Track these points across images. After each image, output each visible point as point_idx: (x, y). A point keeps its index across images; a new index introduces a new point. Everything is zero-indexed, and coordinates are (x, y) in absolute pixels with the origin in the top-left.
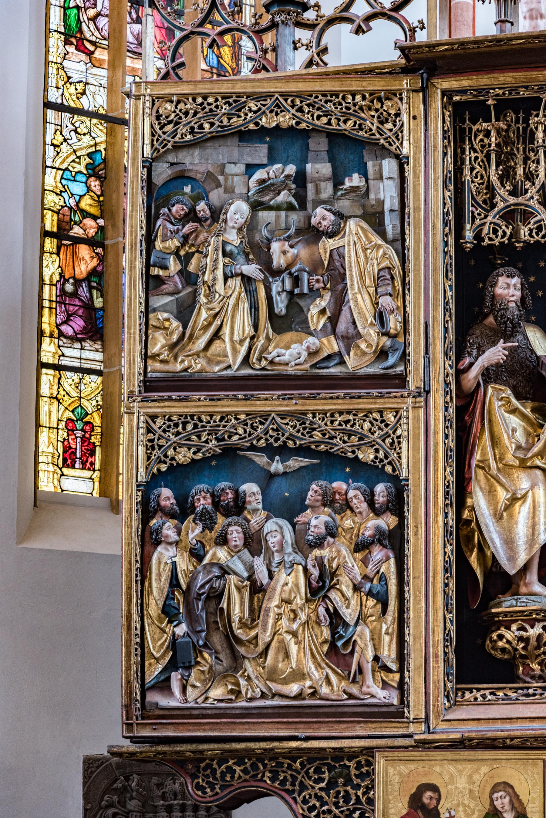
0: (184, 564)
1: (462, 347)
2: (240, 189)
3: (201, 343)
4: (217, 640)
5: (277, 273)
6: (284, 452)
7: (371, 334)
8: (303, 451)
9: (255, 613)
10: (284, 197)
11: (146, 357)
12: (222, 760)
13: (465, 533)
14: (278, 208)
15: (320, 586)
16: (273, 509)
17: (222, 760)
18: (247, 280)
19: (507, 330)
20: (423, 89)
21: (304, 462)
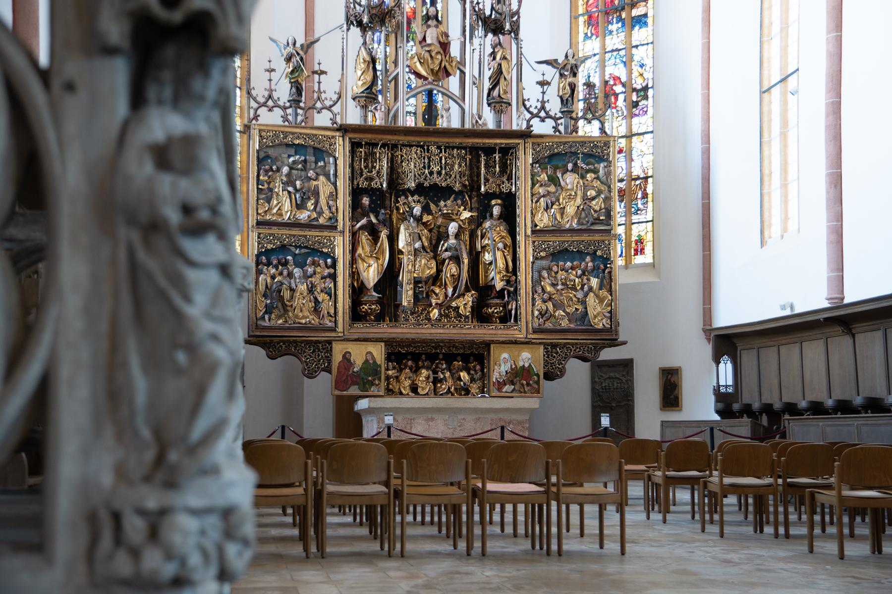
0: (269, 280)
1: (354, 219)
2: (286, 162)
3: (275, 211)
4: (280, 305)
5: (297, 190)
6: (300, 247)
7: (327, 214)
8: (306, 247)
9: (292, 297)
10: (300, 166)
11: (258, 213)
12: (278, 343)
13: (355, 275)
14: (298, 170)
15: (311, 290)
16: (297, 265)
17: (278, 343)
18: (289, 192)
19: (365, 214)
20: (343, 136)
21: (306, 251)
